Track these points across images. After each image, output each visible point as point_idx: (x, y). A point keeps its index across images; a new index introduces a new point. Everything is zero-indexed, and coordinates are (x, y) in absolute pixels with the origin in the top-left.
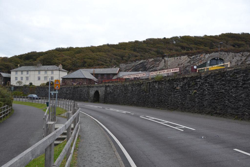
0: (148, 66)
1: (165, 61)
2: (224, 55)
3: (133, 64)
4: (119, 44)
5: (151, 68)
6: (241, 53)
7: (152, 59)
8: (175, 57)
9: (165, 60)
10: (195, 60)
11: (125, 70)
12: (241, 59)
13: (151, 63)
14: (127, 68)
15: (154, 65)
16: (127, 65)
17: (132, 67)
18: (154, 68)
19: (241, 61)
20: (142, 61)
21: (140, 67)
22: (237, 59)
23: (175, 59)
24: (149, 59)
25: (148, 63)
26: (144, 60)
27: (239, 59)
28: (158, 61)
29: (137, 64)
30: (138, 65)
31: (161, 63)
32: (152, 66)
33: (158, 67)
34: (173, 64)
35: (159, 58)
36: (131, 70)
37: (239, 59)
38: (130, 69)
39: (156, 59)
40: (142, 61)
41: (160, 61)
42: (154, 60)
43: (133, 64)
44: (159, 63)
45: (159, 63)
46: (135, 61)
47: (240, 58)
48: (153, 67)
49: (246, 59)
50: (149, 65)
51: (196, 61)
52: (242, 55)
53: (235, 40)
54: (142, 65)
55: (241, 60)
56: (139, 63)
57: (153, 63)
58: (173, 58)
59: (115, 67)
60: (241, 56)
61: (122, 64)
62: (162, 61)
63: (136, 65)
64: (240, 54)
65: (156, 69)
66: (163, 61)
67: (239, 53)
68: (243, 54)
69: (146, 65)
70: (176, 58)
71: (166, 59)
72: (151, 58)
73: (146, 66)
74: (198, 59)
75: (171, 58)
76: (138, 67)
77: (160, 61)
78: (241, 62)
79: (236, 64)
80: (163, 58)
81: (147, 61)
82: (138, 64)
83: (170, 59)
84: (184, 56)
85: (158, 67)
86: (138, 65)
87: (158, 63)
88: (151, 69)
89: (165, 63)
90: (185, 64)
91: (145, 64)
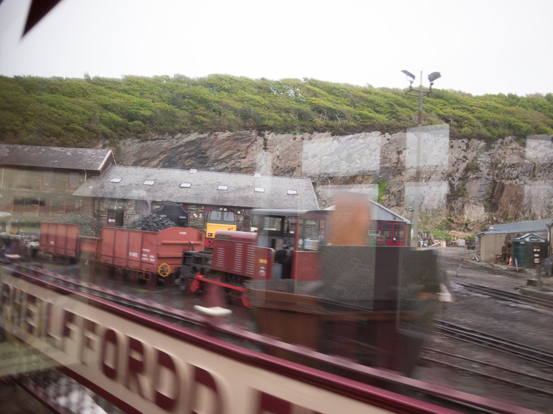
0: (214, 155)
1: (265, 144)
2: (427, 141)
3: (165, 144)
4: (123, 80)
5: (222, 161)
6: (466, 141)
7: (228, 134)
8: (295, 134)
10: (352, 148)
11: (134, 160)
12: (465, 157)
13: (224, 144)
14: (145, 155)
15: (231, 152)
16: (145, 144)
17: (162, 153)
18: (233, 162)
19: (464, 161)
20: (193, 136)
21: (186, 154)
22: (457, 155)
23: (295, 139)
24: (216, 133)
25: (213, 145)
26: (202, 133)
27: (461, 157)
28: (246, 141)
29: (178, 145)
30: (182, 149)
31: (254, 147)
33: (244, 158)
34: (288, 155)
35: (248, 132)
36: (158, 160)
37: (461, 157)
38: (154, 158)
39: (240, 135)
40: (193, 136)
41: (250, 140)
42: (234, 135)
43: (165, 144)
44: (248, 147)
45: (248, 147)
46: (172, 134)
47: (463, 153)
48: (230, 157)
49: (476, 158)
51: (355, 150)
52: (468, 146)
53: (445, 105)
54: (193, 148)
55: (465, 159)
56: (186, 140)
57: (227, 147)
58: (291, 136)
60: (465, 148)
61: (129, 141)
62: (256, 140)
63: (172, 148)
64: (463, 142)
65: (238, 165)
66: (260, 141)
67: (460, 141)
68: (470, 144)
69: (207, 150)
70: (299, 137)
71: (270, 136)
72: (223, 130)
73: (208, 154)
74: (361, 147)
75: (284, 136)
76: (181, 152)
77: (253, 142)
78: (465, 165)
79: (455, 169)
80: (260, 135)
81: (212, 137)
82: (181, 142)
83: (280, 137)
84: (321, 134)
85: (245, 160)
86: (181, 146)
87: (245, 145)
90: (325, 157)
91: (205, 146)
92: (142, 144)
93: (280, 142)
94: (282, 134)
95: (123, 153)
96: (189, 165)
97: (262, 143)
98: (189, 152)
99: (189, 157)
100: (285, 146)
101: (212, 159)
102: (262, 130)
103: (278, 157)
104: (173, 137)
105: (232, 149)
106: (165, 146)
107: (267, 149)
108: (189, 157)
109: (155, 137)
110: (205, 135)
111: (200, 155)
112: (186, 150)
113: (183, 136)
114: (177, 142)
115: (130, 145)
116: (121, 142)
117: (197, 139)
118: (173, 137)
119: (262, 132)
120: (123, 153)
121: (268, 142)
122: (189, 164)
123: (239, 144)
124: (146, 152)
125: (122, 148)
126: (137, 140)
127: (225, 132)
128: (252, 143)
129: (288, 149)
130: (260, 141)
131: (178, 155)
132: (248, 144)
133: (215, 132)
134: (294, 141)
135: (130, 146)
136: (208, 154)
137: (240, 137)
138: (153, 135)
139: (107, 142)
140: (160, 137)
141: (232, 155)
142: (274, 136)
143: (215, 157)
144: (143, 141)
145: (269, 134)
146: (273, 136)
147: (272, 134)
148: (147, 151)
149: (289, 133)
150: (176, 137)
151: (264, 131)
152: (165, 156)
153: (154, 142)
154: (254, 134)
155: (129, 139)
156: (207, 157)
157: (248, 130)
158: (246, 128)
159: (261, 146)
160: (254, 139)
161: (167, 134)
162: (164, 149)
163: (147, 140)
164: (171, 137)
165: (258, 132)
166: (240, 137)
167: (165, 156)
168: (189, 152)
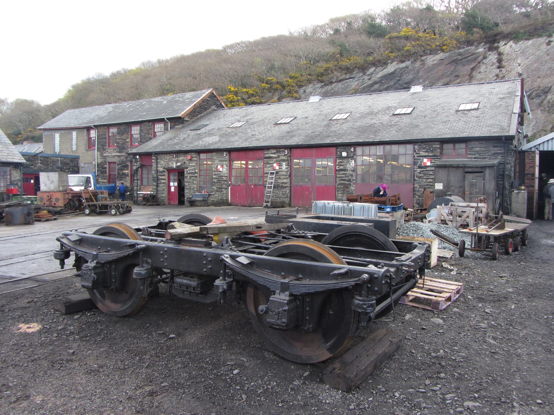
1: (500, 61)
7: (441, 55)
9: (500, 54)
16: (329, 88)
20: (391, 68)
23: (549, 43)
24: (423, 58)
25: (420, 74)
26: (402, 62)
29: (370, 82)
31: (482, 68)
34: (538, 69)
39: (460, 54)
44: (473, 69)
45: (473, 69)
46: (363, 69)
56: (380, 75)
58: (543, 40)
59: (276, 99)
62: (485, 58)
66: (493, 57)
71: (507, 48)
72: (433, 52)
75: (530, 42)
81: (418, 64)
86: (375, 83)
87: (468, 68)
89: (499, 67)
93: (523, 53)
94: (526, 39)
97: (495, 61)
100: (531, 58)
102: (495, 41)
103: (520, 75)
104: (364, 74)
105: (448, 76)
106: (353, 86)
107: (503, 67)
109: (342, 78)
110: (408, 63)
113: (377, 70)
114: (369, 79)
117: (396, 70)
118: (364, 74)
119: (496, 45)
121: (504, 57)
123: (459, 67)
126: (319, 85)
127: (437, 54)
128: (479, 63)
129: (535, 62)
130: (493, 57)
132: (472, 66)
133: (421, 56)
134: (549, 47)
137: (460, 57)
138: (339, 75)
140: (348, 76)
142: (514, 45)
144: (326, 85)
145: (505, 44)
146: (511, 46)
147: (511, 43)
149: (540, 36)
150: (368, 73)
151: (499, 43)
153: (340, 84)
154: (481, 50)
155: (311, 86)
157: (472, 45)
158: (469, 43)
159: (493, 64)
160: (481, 57)
161: (356, 71)
163: (331, 83)
164: (361, 74)
165: (488, 45)
166: (460, 57)
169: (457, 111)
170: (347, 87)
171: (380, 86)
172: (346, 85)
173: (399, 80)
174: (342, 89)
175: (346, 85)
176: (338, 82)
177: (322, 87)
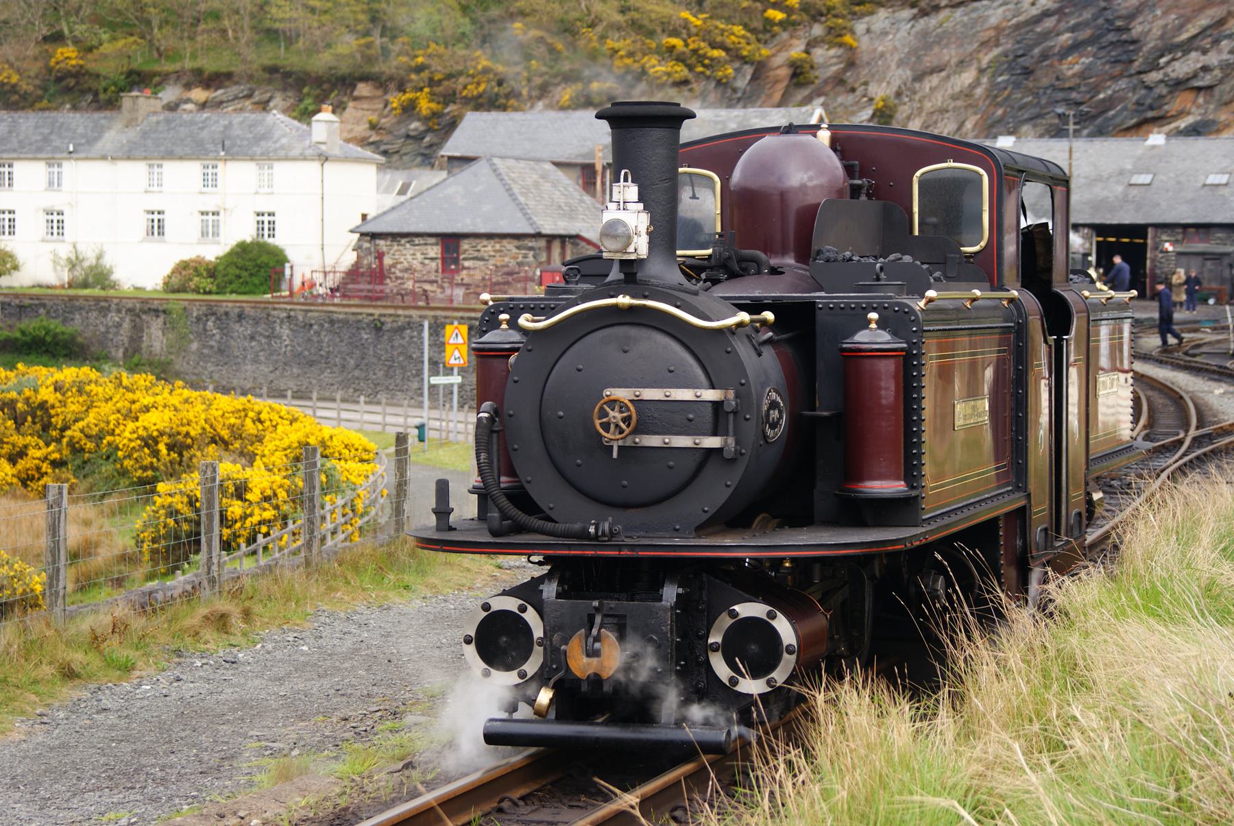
0: (1156, 32)
5: (1187, 47)
14: (929, 61)
16: (932, 21)
29: (1034, 11)
30: (1049, 23)
32: (1204, 21)
50: (1165, 13)
63: (1018, 26)
69: (1131, 17)
73: (1137, 29)
76: (1046, 35)
86: (1046, 14)
88: (1186, 52)
92: (922, 22)
95: (866, 58)
96: (1074, 76)
98: (1073, 29)
99: (1075, 47)
101: (1151, 44)
106: (993, 21)
108: (1075, 47)
111: (1112, 37)
112: (1063, 25)
115: (885, 33)
116: (860, 27)
120: (866, 58)
122: (1077, 68)
124: (936, 49)
125: (864, 43)
126: (907, 13)
131: (1037, 44)
135: (887, 33)
136: (1137, 29)
139: (818, 30)
141: (1221, 22)
143: (1162, 37)
144: (924, 13)
148: (938, 43)
152: (996, 51)
155: (882, 13)
156: (1134, 42)
162: (992, 33)
167: (996, 51)
168: (1073, 29)
169: (1205, 185)
170: (976, 21)
171: (1059, 21)
172: (974, 15)
173: (1105, 9)
174: (965, 25)
175: (974, 15)
176: (953, 6)
177: (914, 18)
